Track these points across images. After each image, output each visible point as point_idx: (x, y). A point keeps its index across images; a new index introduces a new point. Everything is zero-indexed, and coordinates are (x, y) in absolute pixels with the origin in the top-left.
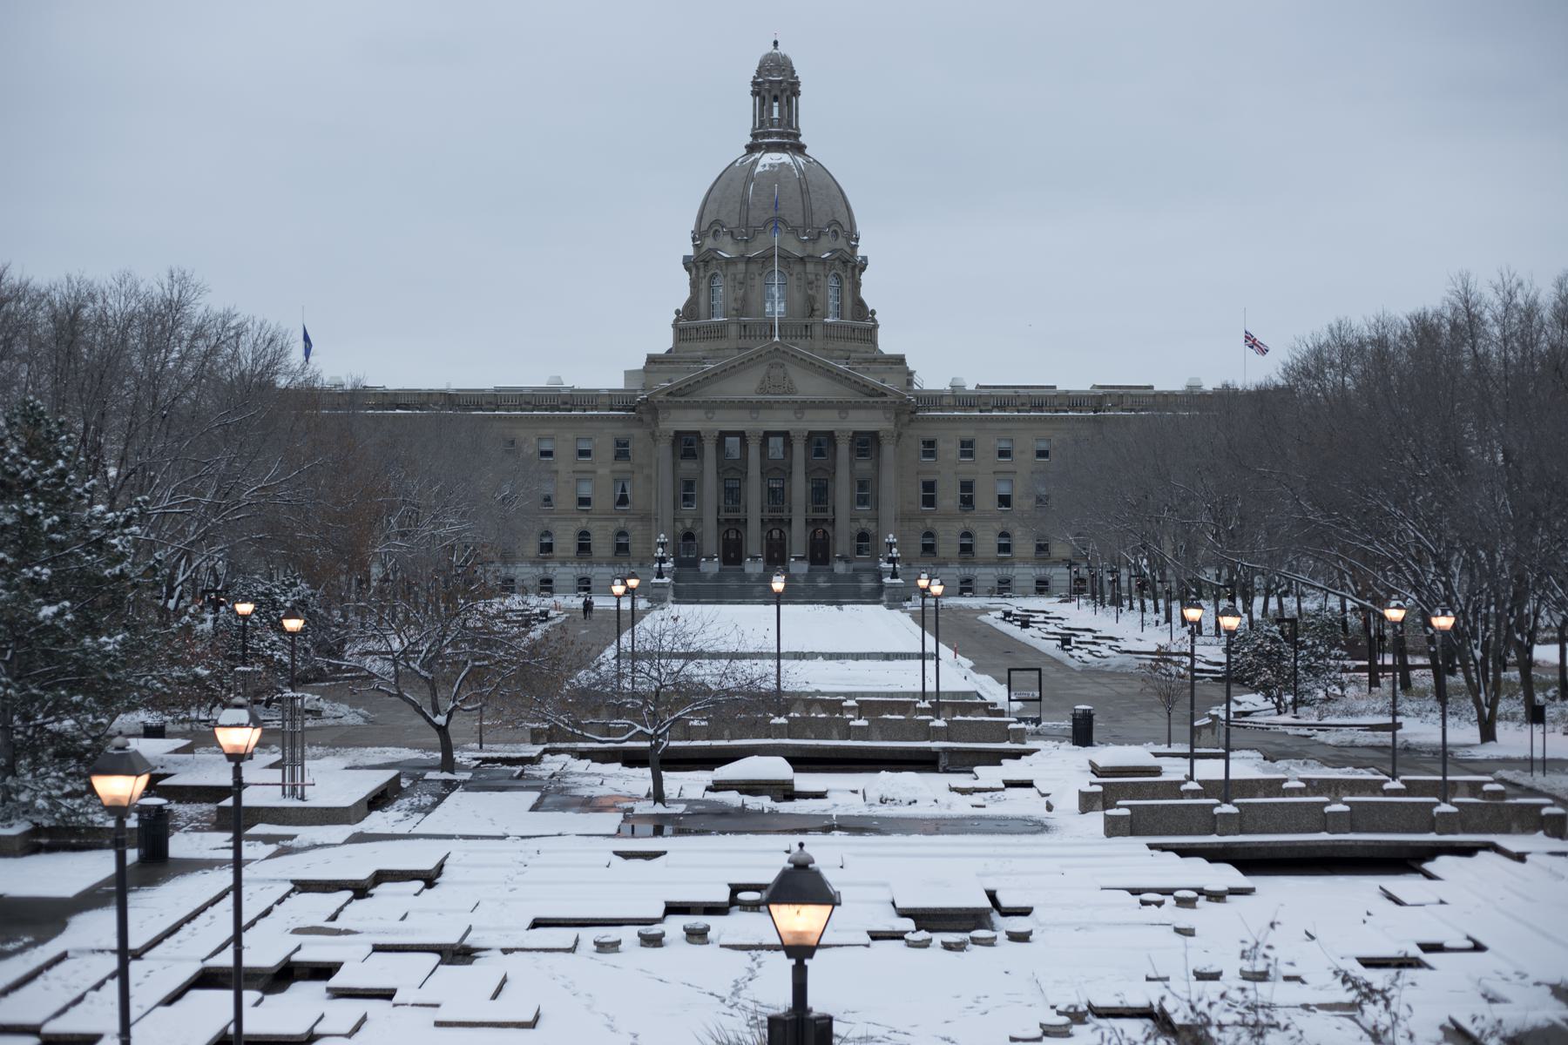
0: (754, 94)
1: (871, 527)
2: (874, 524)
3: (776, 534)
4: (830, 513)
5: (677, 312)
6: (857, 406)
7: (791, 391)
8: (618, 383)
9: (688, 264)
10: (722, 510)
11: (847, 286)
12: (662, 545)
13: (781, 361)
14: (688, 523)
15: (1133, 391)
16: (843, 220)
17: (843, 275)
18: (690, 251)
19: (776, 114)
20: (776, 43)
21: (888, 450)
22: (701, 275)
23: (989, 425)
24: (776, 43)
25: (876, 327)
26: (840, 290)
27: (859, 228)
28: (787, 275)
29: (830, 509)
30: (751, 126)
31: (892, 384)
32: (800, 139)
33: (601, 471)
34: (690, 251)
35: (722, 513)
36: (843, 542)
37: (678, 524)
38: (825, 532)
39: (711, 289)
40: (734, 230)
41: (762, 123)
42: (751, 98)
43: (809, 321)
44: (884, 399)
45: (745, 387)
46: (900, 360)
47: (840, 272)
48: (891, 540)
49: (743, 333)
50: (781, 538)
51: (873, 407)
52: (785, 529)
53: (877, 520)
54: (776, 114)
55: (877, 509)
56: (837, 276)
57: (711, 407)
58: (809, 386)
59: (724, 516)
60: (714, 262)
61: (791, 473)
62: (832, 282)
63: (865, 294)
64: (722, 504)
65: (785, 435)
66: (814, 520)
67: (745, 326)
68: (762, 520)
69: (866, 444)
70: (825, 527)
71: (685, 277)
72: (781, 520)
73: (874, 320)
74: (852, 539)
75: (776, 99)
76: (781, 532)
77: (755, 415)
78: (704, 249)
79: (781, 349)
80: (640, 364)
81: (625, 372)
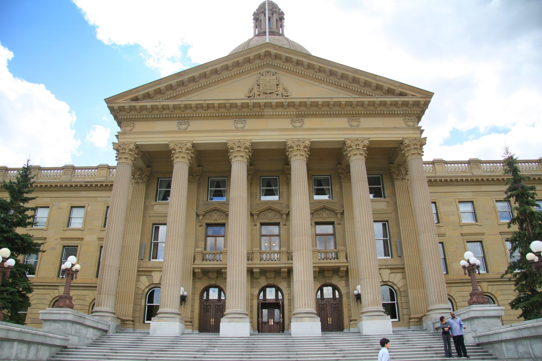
4: (342, 259)
13: (274, 71)
33: (87, 238)
35: (198, 261)
44: (405, 99)
52: (283, 285)
53: (401, 269)
59: (200, 264)
61: (288, 214)
72: (277, 272)
77: (240, 126)
79: (273, 51)
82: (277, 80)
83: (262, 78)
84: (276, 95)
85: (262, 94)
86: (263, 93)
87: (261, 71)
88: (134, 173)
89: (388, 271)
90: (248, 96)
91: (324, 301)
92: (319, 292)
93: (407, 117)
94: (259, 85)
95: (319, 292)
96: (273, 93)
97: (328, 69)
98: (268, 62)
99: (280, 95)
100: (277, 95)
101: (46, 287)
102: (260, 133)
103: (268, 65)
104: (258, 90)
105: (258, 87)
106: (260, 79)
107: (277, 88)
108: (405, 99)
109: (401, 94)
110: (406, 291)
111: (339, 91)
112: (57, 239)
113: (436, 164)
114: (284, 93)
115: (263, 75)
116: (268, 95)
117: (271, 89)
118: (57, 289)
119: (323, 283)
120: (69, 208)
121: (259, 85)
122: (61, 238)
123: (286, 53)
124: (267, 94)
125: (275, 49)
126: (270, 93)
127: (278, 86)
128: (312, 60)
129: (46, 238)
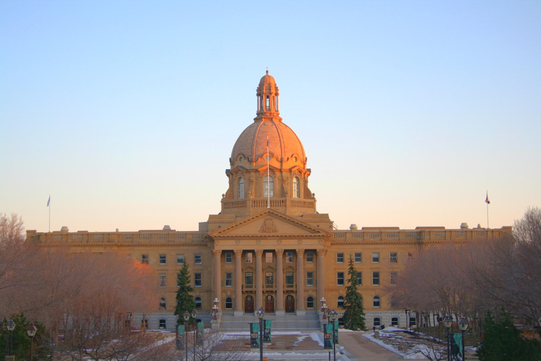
0: (258, 95)
1: (313, 294)
2: (315, 293)
3: (269, 298)
5: (223, 195)
6: (307, 237)
7: (275, 231)
8: (196, 229)
9: (228, 172)
10: (244, 287)
11: (302, 182)
12: (216, 303)
13: (270, 217)
14: (229, 293)
15: (387, 231)
16: (300, 152)
17: (299, 178)
18: (229, 167)
19: (268, 105)
20: (267, 72)
21: (322, 257)
22: (234, 178)
23: (368, 246)
24: (267, 72)
25: (315, 201)
26: (298, 185)
27: (307, 154)
28: (273, 177)
29: (294, 286)
30: (257, 110)
31: (323, 226)
32: (279, 116)
34: (229, 167)
36: (301, 301)
37: (224, 294)
38: (292, 297)
39: (239, 184)
40: (249, 157)
41: (262, 107)
42: (256, 97)
43: (283, 199)
45: (254, 228)
46: (326, 216)
47: (298, 176)
48: (323, 300)
49: (254, 205)
50: (272, 300)
51: (314, 237)
54: (268, 105)
55: (317, 286)
56: (297, 178)
57: (237, 238)
58: (284, 229)
59: (245, 289)
60: (240, 172)
62: (295, 180)
63: (310, 186)
64: (244, 284)
65: (273, 251)
66: (287, 291)
67: (254, 201)
68: (263, 291)
69: (311, 254)
70: (293, 294)
71: (227, 179)
72: (272, 291)
73: (314, 198)
74: (305, 300)
75: (268, 97)
76: (272, 297)
78: (235, 166)
79: (271, 212)
80: (206, 219)
81: (200, 224)
87: (266, 217)
89: (311, 291)
103: (269, 215)
109: (318, 232)
110: (317, 299)
113: (347, 234)
119: (288, 295)
121: (265, 225)
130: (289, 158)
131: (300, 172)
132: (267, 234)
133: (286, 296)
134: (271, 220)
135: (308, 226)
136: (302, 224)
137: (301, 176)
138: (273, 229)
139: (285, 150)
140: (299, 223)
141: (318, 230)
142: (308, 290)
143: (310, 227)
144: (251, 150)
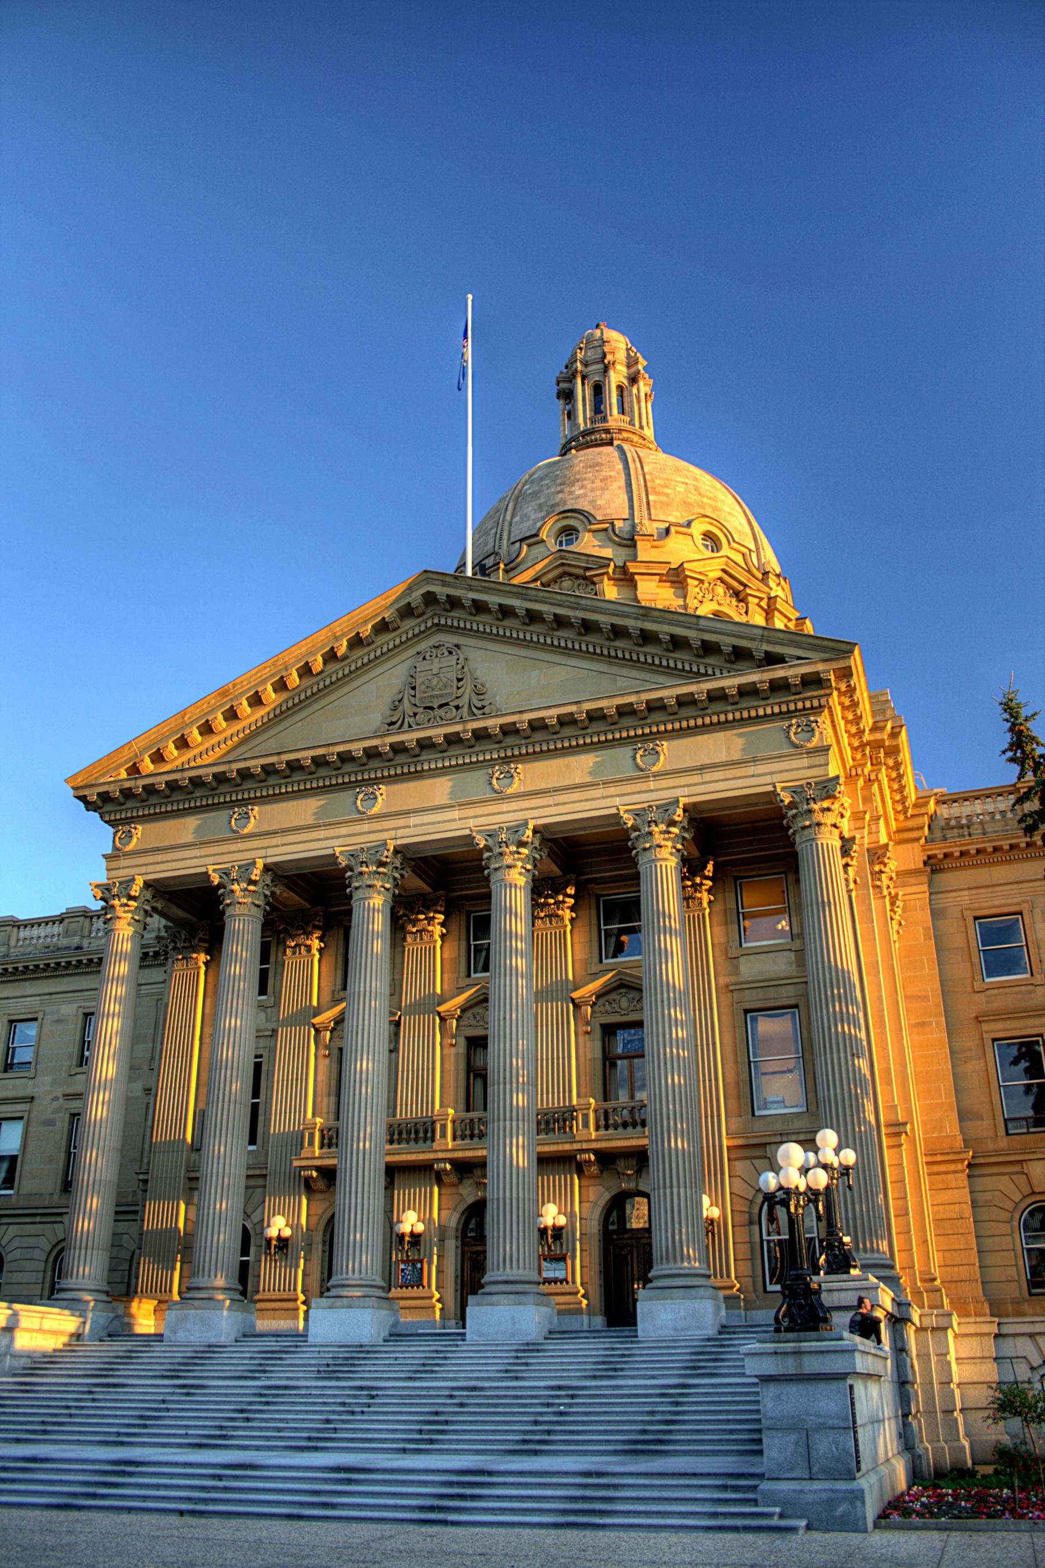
13: (450, 639)
44: (779, 672)
66: (607, 1159)
82: (460, 667)
83: (422, 666)
84: (454, 710)
85: (421, 710)
86: (425, 708)
87: (423, 646)
88: (175, 936)
90: (389, 721)
91: (626, 1236)
92: (614, 1214)
93: (794, 721)
94: (414, 688)
95: (614, 1214)
96: (447, 704)
97: (576, 618)
98: (436, 621)
99: (465, 709)
100: (457, 708)
101: (38, 1219)
102: (413, 820)
104: (413, 700)
105: (412, 692)
106: (418, 670)
107: (458, 688)
108: (779, 672)
109: (772, 659)
111: (614, 670)
112: (56, 1099)
114: (475, 701)
115: (424, 658)
116: (437, 712)
117: (442, 696)
118: (61, 1222)
120: (81, 1017)
121: (414, 688)
122: (64, 1095)
123: (471, 590)
124: (432, 708)
125: (444, 584)
126: (441, 706)
127: (460, 685)
128: (536, 601)
129: (33, 1098)
130: (673, 529)
131: (736, 594)
132: (410, 737)
133: (600, 1194)
134: (450, 653)
135: (691, 634)
136: (650, 626)
137: (746, 613)
138: (464, 702)
139: (651, 498)
140: (630, 623)
141: (766, 647)
142: (764, 1145)
143: (707, 637)
144: (494, 531)
